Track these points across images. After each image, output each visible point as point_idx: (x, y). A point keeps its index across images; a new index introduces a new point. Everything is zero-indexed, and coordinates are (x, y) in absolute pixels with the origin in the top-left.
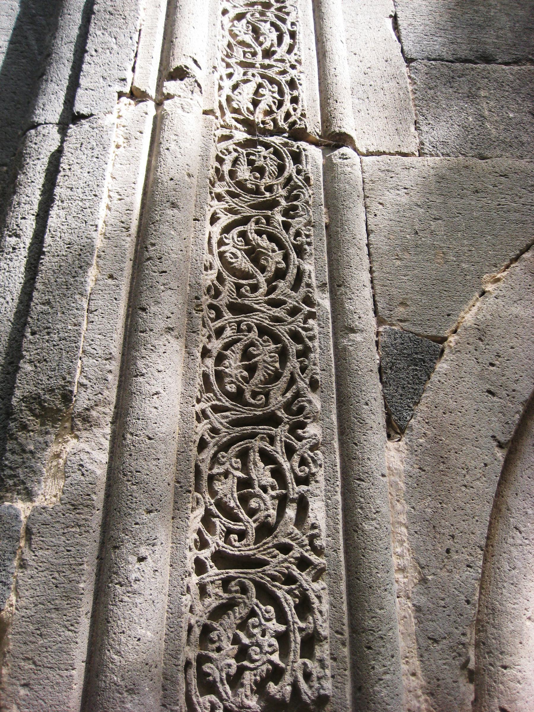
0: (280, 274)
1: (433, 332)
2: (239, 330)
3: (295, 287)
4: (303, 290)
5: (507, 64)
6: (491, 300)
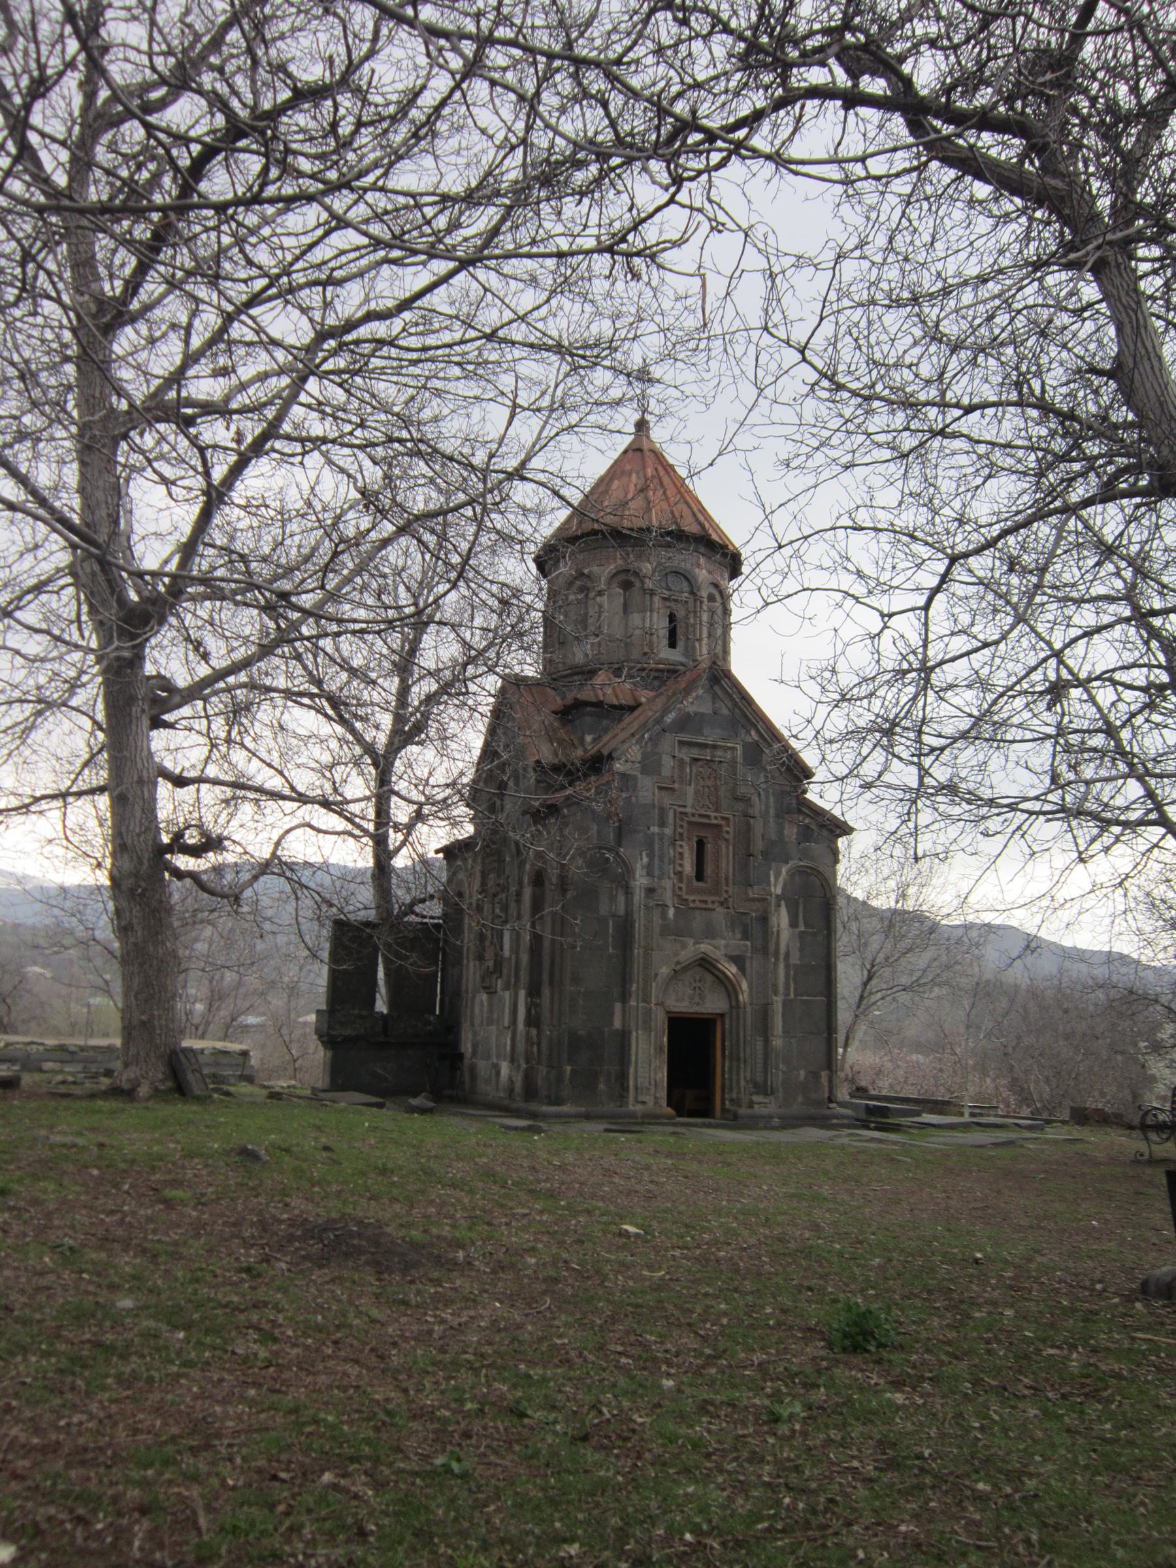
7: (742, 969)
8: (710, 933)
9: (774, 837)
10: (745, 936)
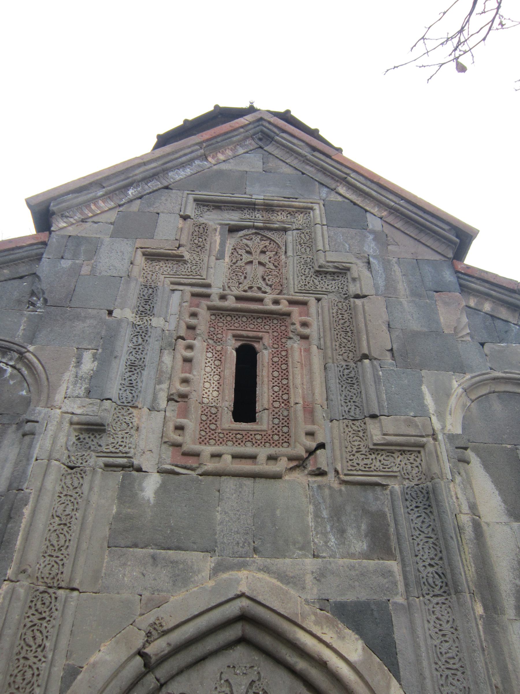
0: (40, 646)
1: (80, 665)
2: (23, 667)
3: (42, 651)
4: (44, 653)
5: (142, 548)
6: (101, 653)
7: (384, 648)
8: (266, 540)
9: (415, 326)
10: (380, 542)
